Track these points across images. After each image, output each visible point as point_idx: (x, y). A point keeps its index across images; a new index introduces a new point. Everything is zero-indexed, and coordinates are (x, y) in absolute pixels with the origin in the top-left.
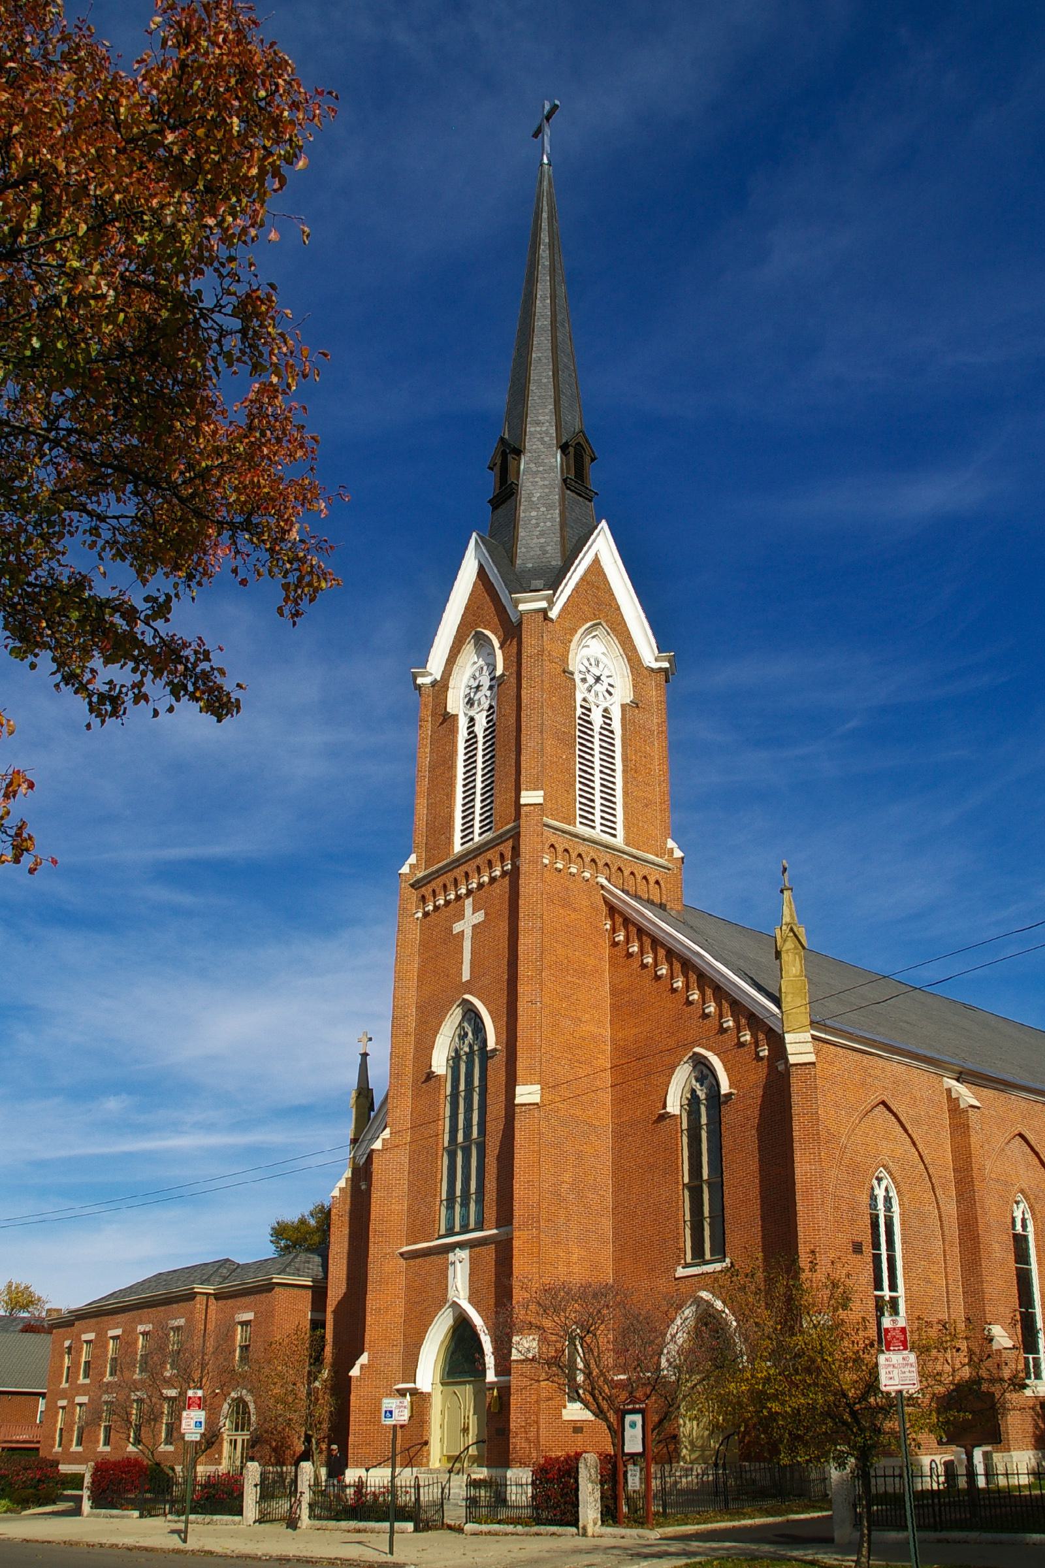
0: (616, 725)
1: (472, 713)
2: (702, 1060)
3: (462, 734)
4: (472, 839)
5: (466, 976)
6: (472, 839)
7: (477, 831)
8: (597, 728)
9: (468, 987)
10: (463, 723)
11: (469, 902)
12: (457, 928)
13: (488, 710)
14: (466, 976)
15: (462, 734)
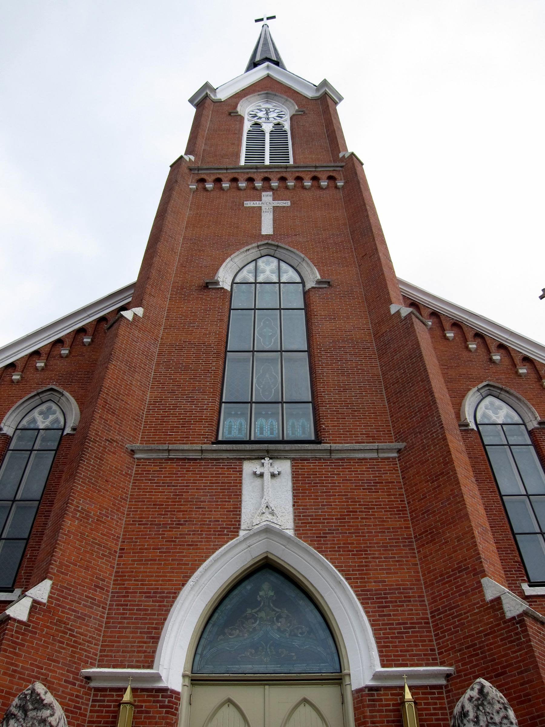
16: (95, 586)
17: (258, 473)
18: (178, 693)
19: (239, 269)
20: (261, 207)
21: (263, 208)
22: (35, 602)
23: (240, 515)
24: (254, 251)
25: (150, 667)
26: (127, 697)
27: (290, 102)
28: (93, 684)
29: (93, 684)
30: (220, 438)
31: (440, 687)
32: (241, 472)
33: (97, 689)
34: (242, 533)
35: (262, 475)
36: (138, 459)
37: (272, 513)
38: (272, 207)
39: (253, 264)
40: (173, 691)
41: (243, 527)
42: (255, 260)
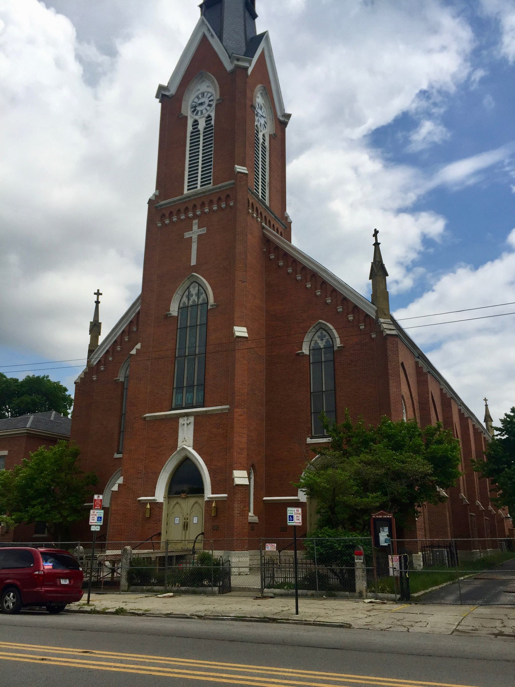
0: (267, 144)
1: (197, 118)
2: (324, 327)
3: (190, 129)
4: (196, 187)
5: (193, 262)
6: (196, 187)
7: (199, 184)
8: (260, 144)
9: (195, 269)
10: (190, 122)
11: (195, 222)
12: (187, 235)
13: (207, 118)
14: (193, 262)
15: (190, 129)
16: (138, 473)
17: (183, 424)
18: (162, 503)
19: (181, 296)
20: (191, 237)
21: (193, 238)
22: (119, 484)
23: (178, 441)
24: (187, 282)
25: (154, 496)
26: (148, 506)
27: (213, 82)
28: (141, 502)
29: (141, 502)
30: (173, 406)
31: (225, 500)
32: (178, 423)
33: (143, 503)
34: (178, 449)
35: (184, 424)
36: (148, 420)
37: (186, 441)
38: (197, 236)
39: (187, 291)
40: (161, 503)
41: (178, 446)
42: (188, 288)
